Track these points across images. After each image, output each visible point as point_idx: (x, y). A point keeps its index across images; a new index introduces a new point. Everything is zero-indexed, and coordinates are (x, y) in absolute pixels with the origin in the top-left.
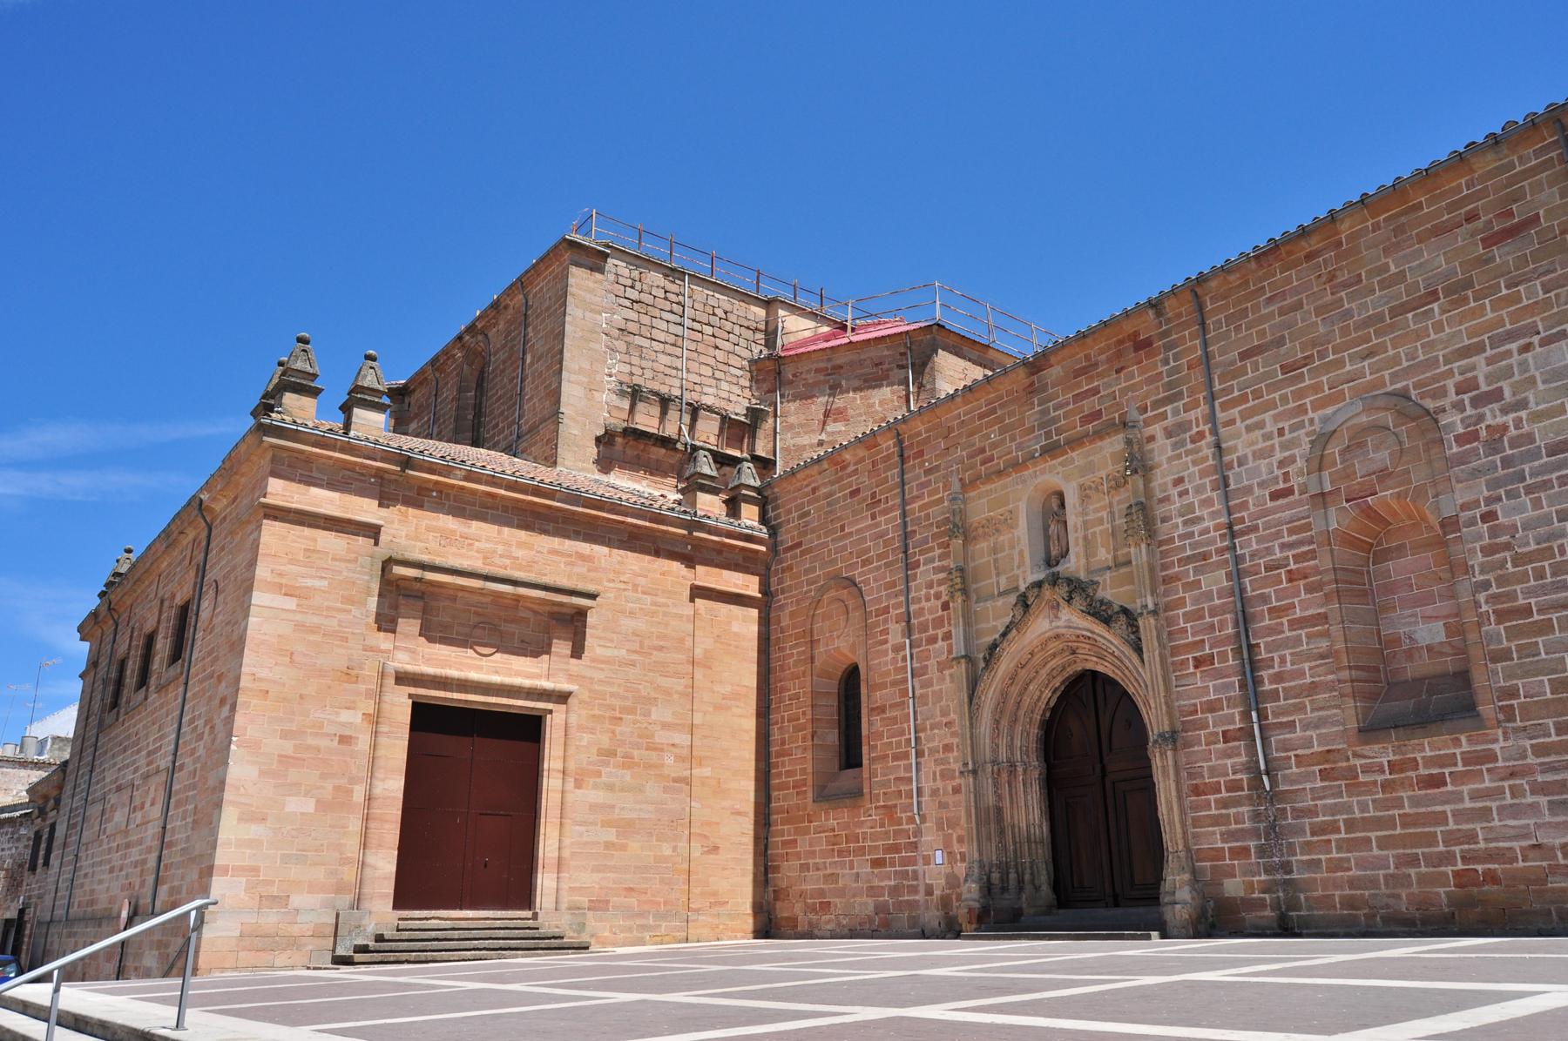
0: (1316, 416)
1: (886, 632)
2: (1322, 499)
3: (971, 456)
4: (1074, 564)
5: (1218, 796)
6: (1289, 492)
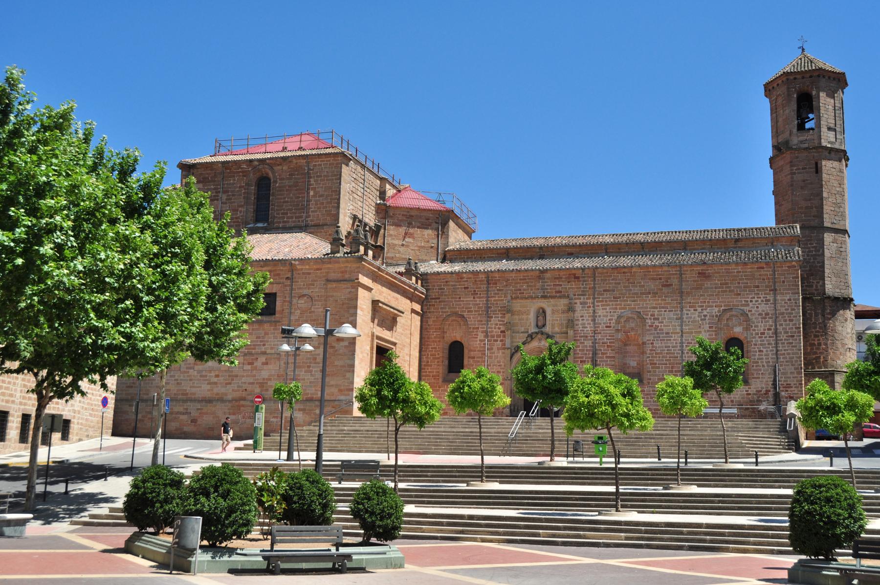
2: (618, 331)
4: (548, 329)
6: (610, 327)
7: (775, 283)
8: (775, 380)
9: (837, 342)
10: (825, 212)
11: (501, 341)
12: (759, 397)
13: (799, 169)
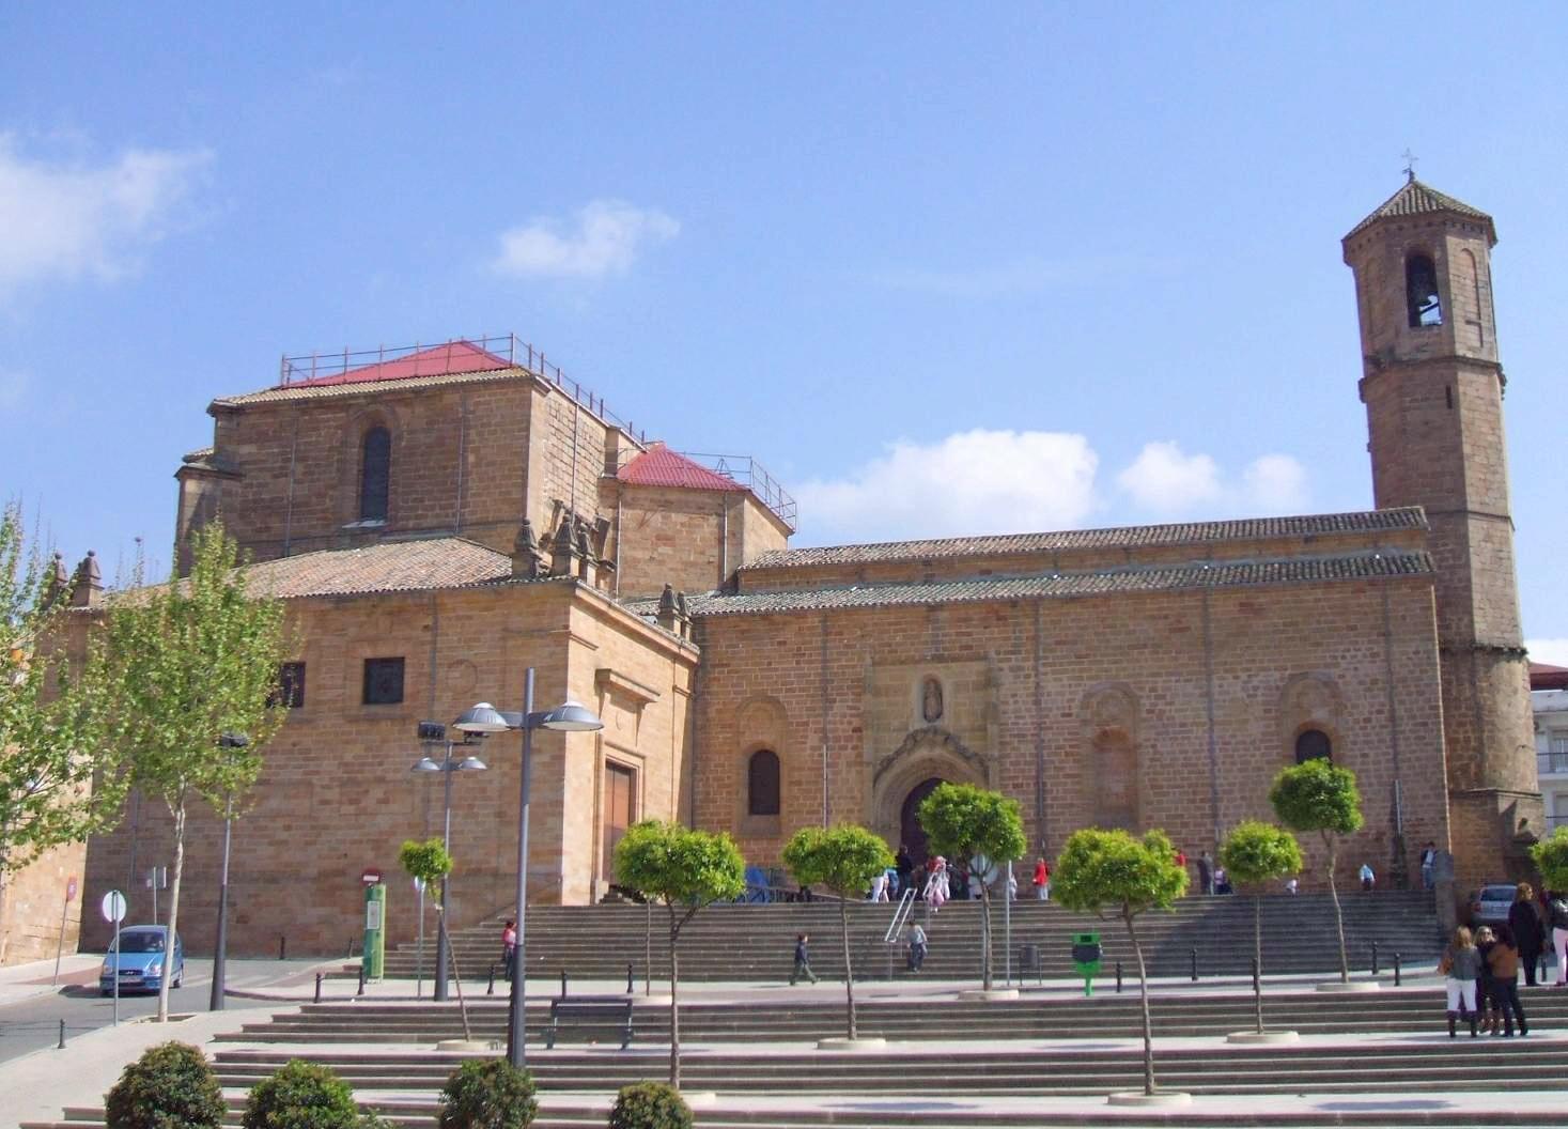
0: (1089, 683)
1: (806, 737)
2: (1085, 722)
3: (881, 645)
4: (947, 722)
6: (1070, 715)
7: (1386, 619)
8: (1393, 813)
9: (1500, 735)
10: (1468, 482)
11: (854, 748)
12: (1363, 847)
13: (1416, 400)
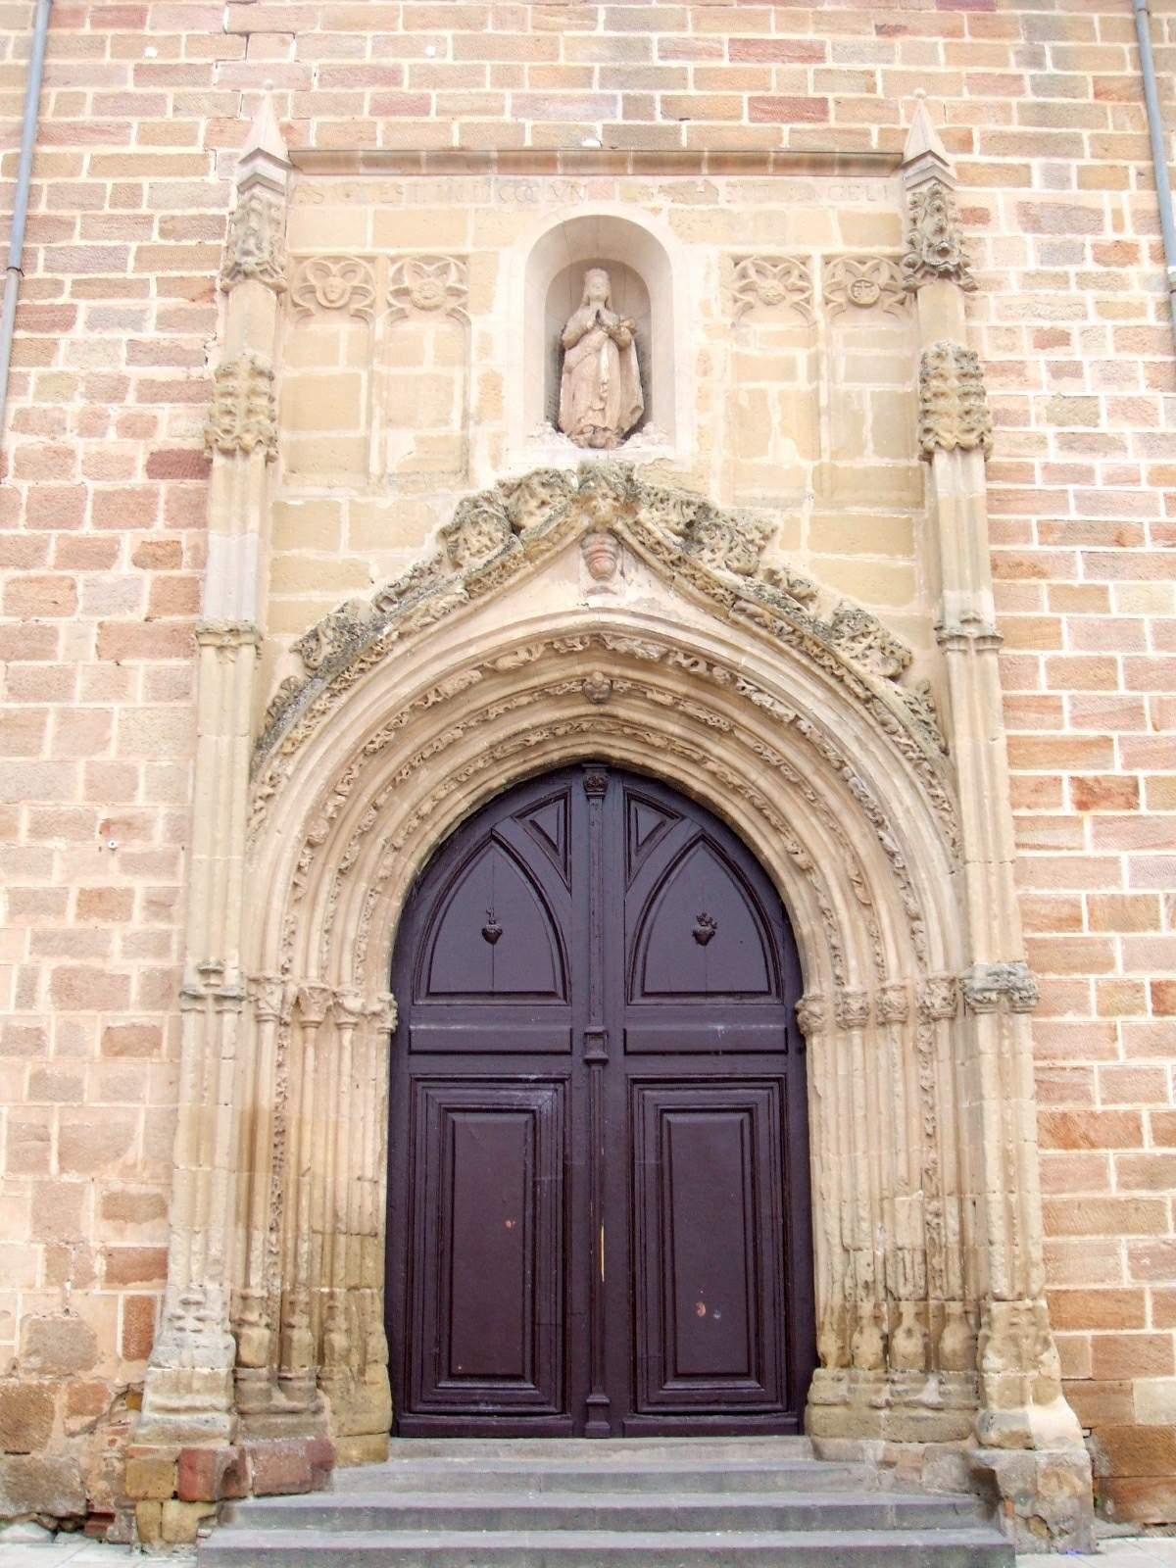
5: (1131, 1153)
11: (150, 557)
